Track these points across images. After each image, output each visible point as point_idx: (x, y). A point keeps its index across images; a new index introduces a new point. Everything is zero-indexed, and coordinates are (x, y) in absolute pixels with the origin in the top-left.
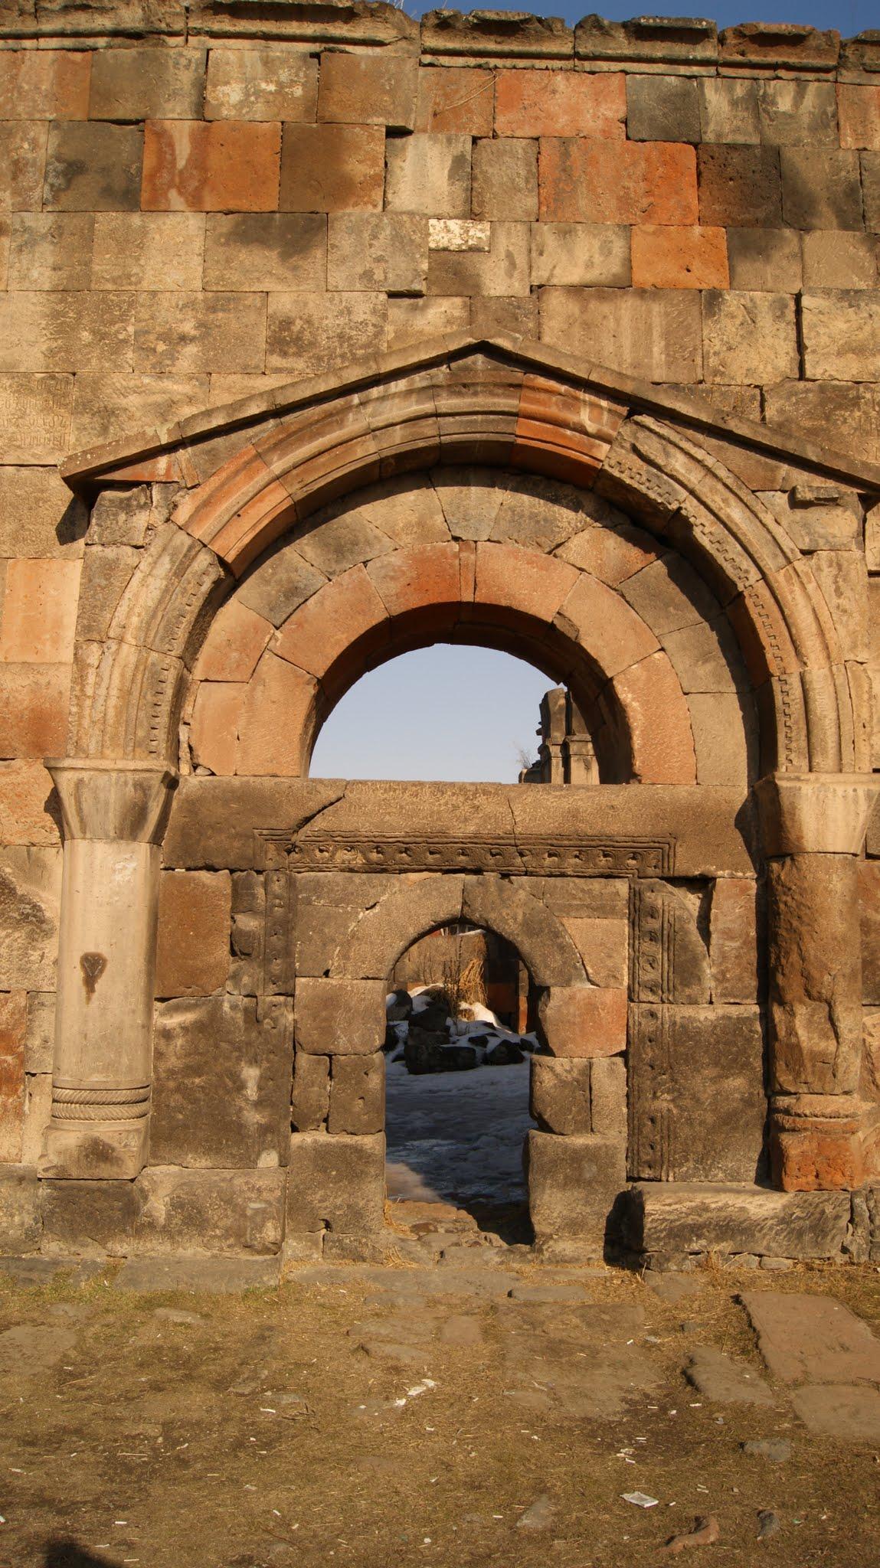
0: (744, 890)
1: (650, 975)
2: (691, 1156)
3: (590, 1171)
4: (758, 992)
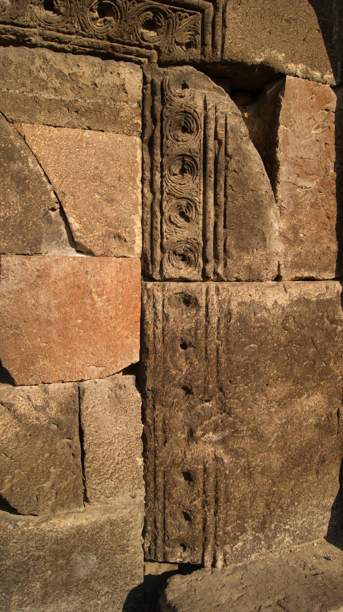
0: (323, 100)
1: (184, 232)
2: (250, 523)
3: (86, 565)
4: (338, 261)
